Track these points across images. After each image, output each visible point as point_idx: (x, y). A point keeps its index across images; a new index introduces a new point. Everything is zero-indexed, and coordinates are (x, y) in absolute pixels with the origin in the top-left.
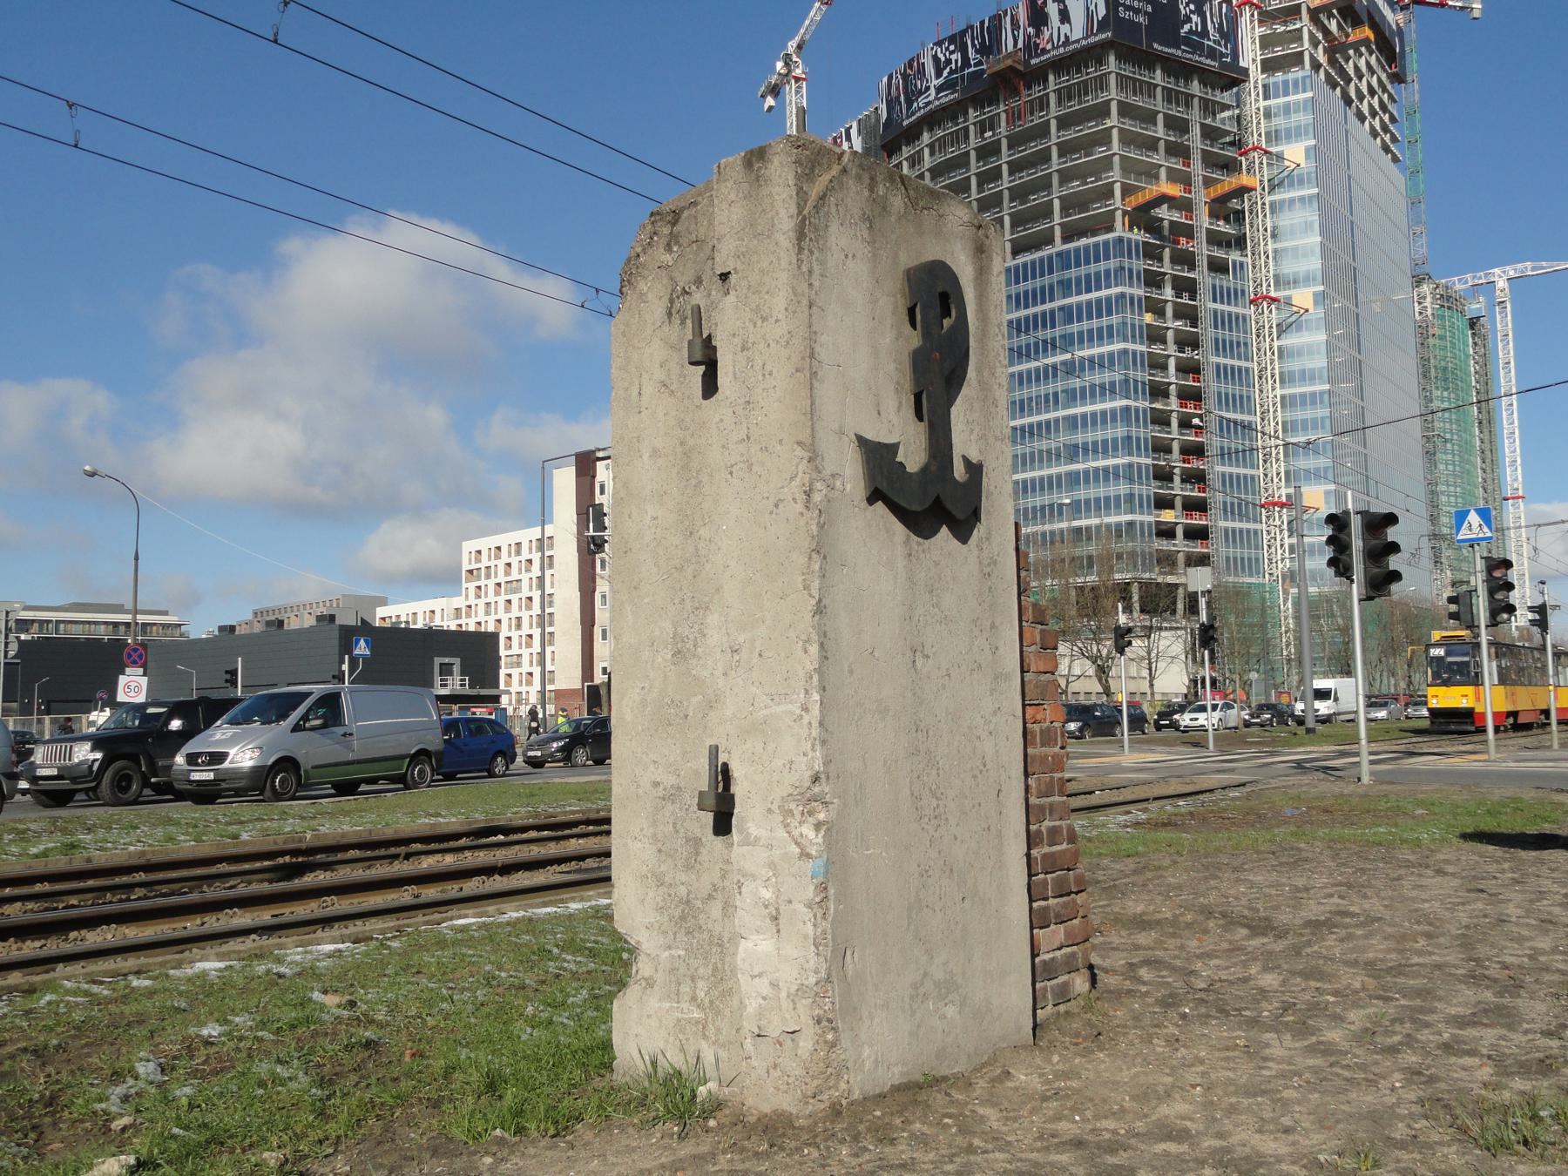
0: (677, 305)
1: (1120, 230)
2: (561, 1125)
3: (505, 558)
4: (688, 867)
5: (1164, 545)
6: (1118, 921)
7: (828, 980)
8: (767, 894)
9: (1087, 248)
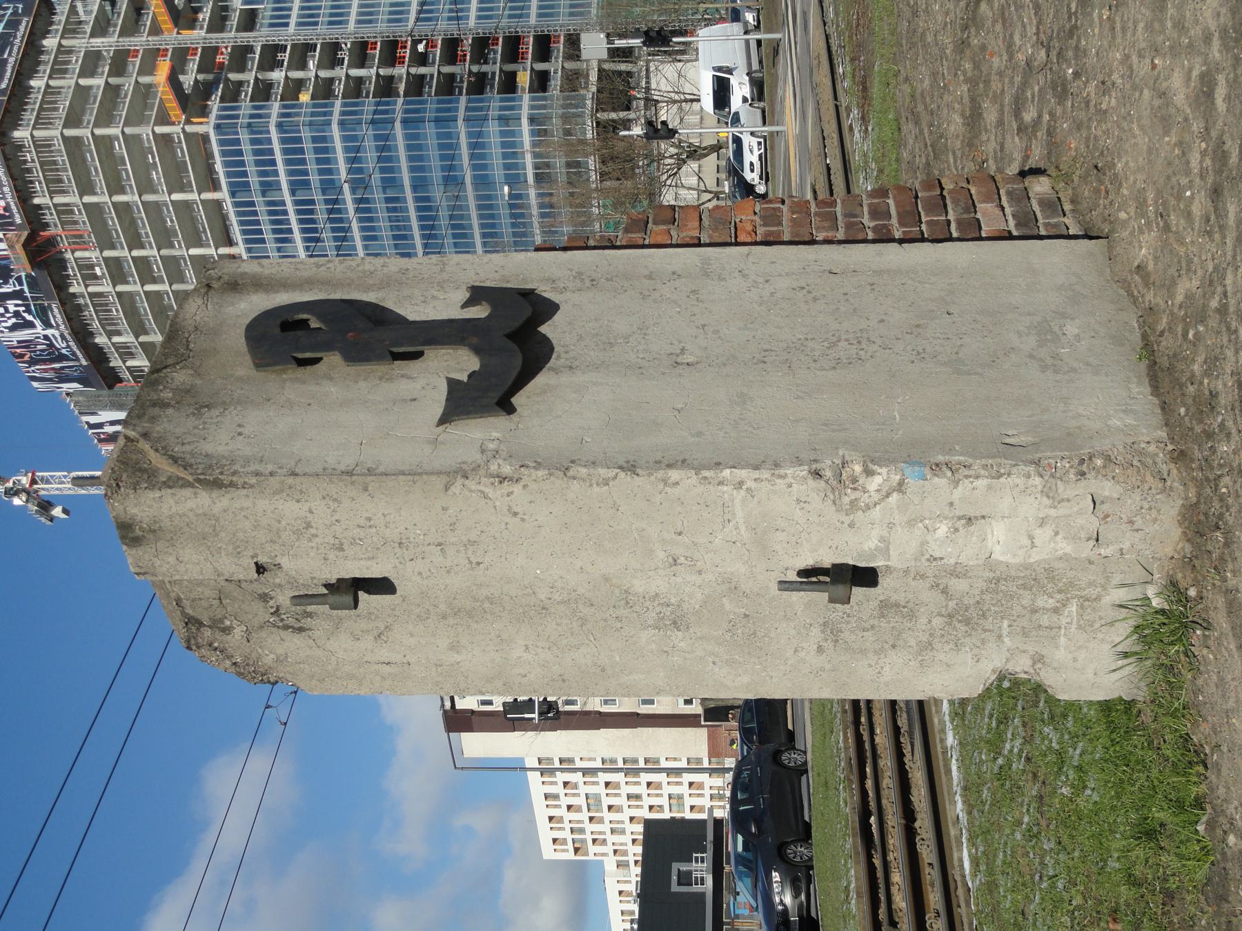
0: (291, 622)
1: (206, 127)
2: (1194, 758)
3: (563, 812)
4: (912, 615)
5: (556, 82)
6: (971, 143)
7: (1037, 463)
8: (943, 529)
9: (226, 164)
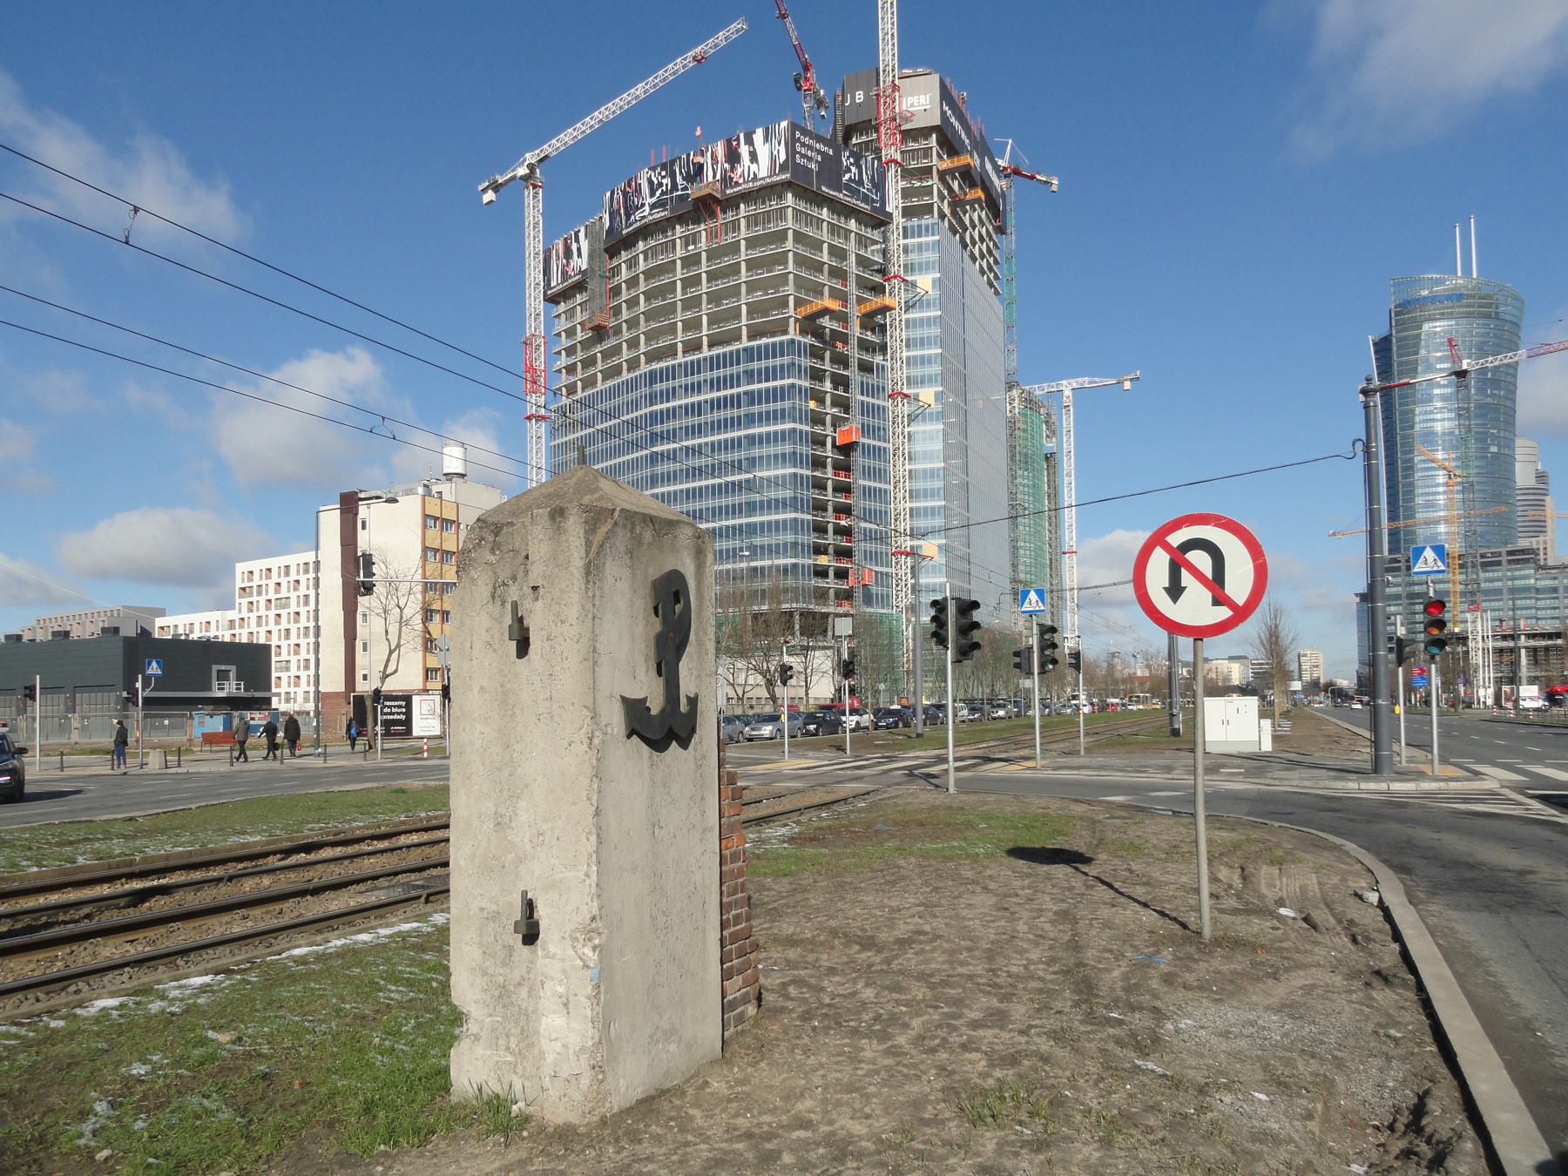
0: (498, 592)
1: (793, 333)
2: (423, 1135)
3: (275, 578)
4: (504, 964)
5: (821, 583)
6: (776, 940)
7: (600, 1042)
8: (561, 989)
9: (766, 346)
